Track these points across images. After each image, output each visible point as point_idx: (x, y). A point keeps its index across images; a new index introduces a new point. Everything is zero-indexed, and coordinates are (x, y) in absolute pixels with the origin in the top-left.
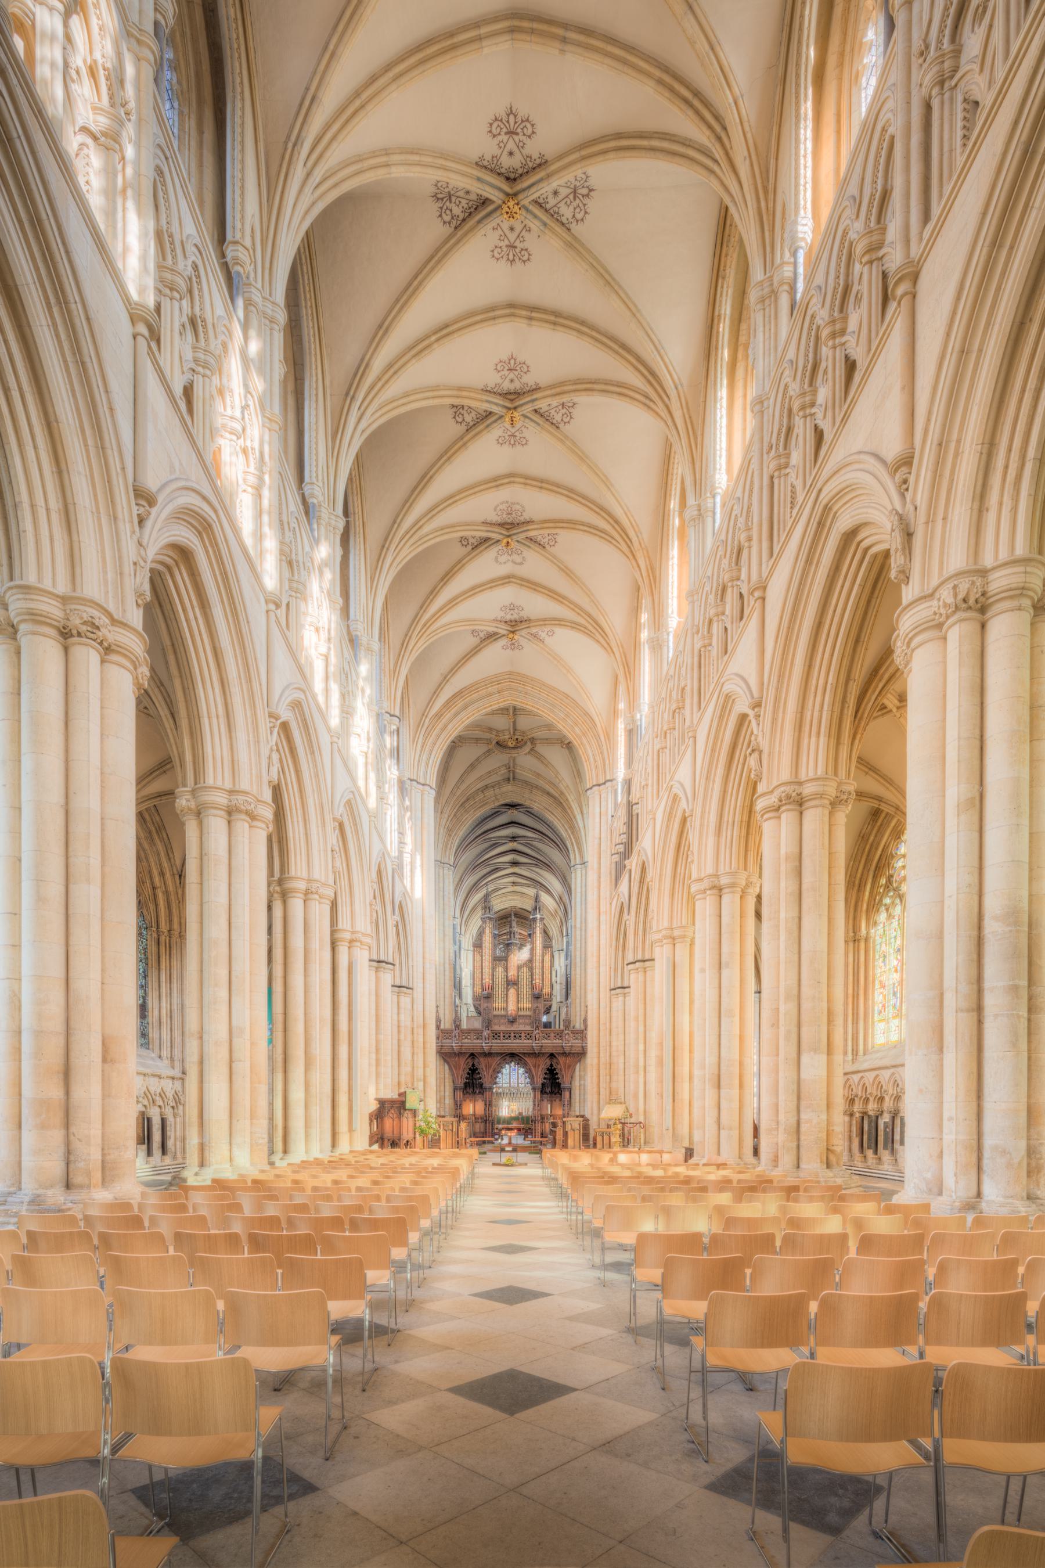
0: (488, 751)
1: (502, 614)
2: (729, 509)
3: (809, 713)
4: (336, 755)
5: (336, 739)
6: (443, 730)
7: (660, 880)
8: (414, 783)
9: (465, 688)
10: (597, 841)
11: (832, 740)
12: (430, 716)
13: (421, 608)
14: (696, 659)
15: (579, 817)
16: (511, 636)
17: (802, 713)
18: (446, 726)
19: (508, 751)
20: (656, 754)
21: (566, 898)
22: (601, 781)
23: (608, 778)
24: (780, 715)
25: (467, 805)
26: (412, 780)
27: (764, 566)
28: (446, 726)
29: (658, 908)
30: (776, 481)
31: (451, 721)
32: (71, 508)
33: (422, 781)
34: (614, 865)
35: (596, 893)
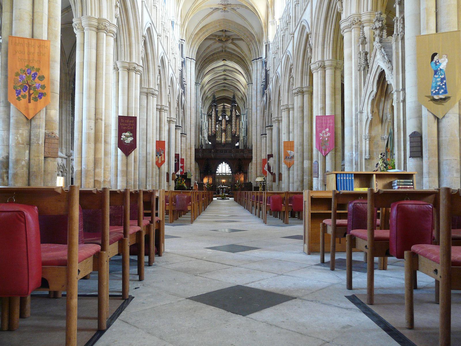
0: (215, 42)
1: (221, 2)
2: (287, 4)
3: (304, 70)
4: (170, 66)
5: (170, 61)
6: (199, 39)
7: (274, 101)
8: (188, 58)
9: (207, 24)
10: (256, 79)
11: (311, 77)
12: (194, 35)
13: (193, 4)
14: (282, 38)
15: (250, 66)
16: (224, 9)
17: (303, 69)
18: (200, 38)
19: (223, 42)
20: (273, 59)
21: (244, 98)
22: (258, 58)
23: (260, 57)
24: (298, 69)
25: (206, 61)
26: (187, 58)
27: (294, 28)
28: (200, 38)
29: (274, 110)
30: (296, 7)
31: (202, 35)
32: (131, 44)
33: (191, 58)
34: (262, 89)
35: (255, 99)
